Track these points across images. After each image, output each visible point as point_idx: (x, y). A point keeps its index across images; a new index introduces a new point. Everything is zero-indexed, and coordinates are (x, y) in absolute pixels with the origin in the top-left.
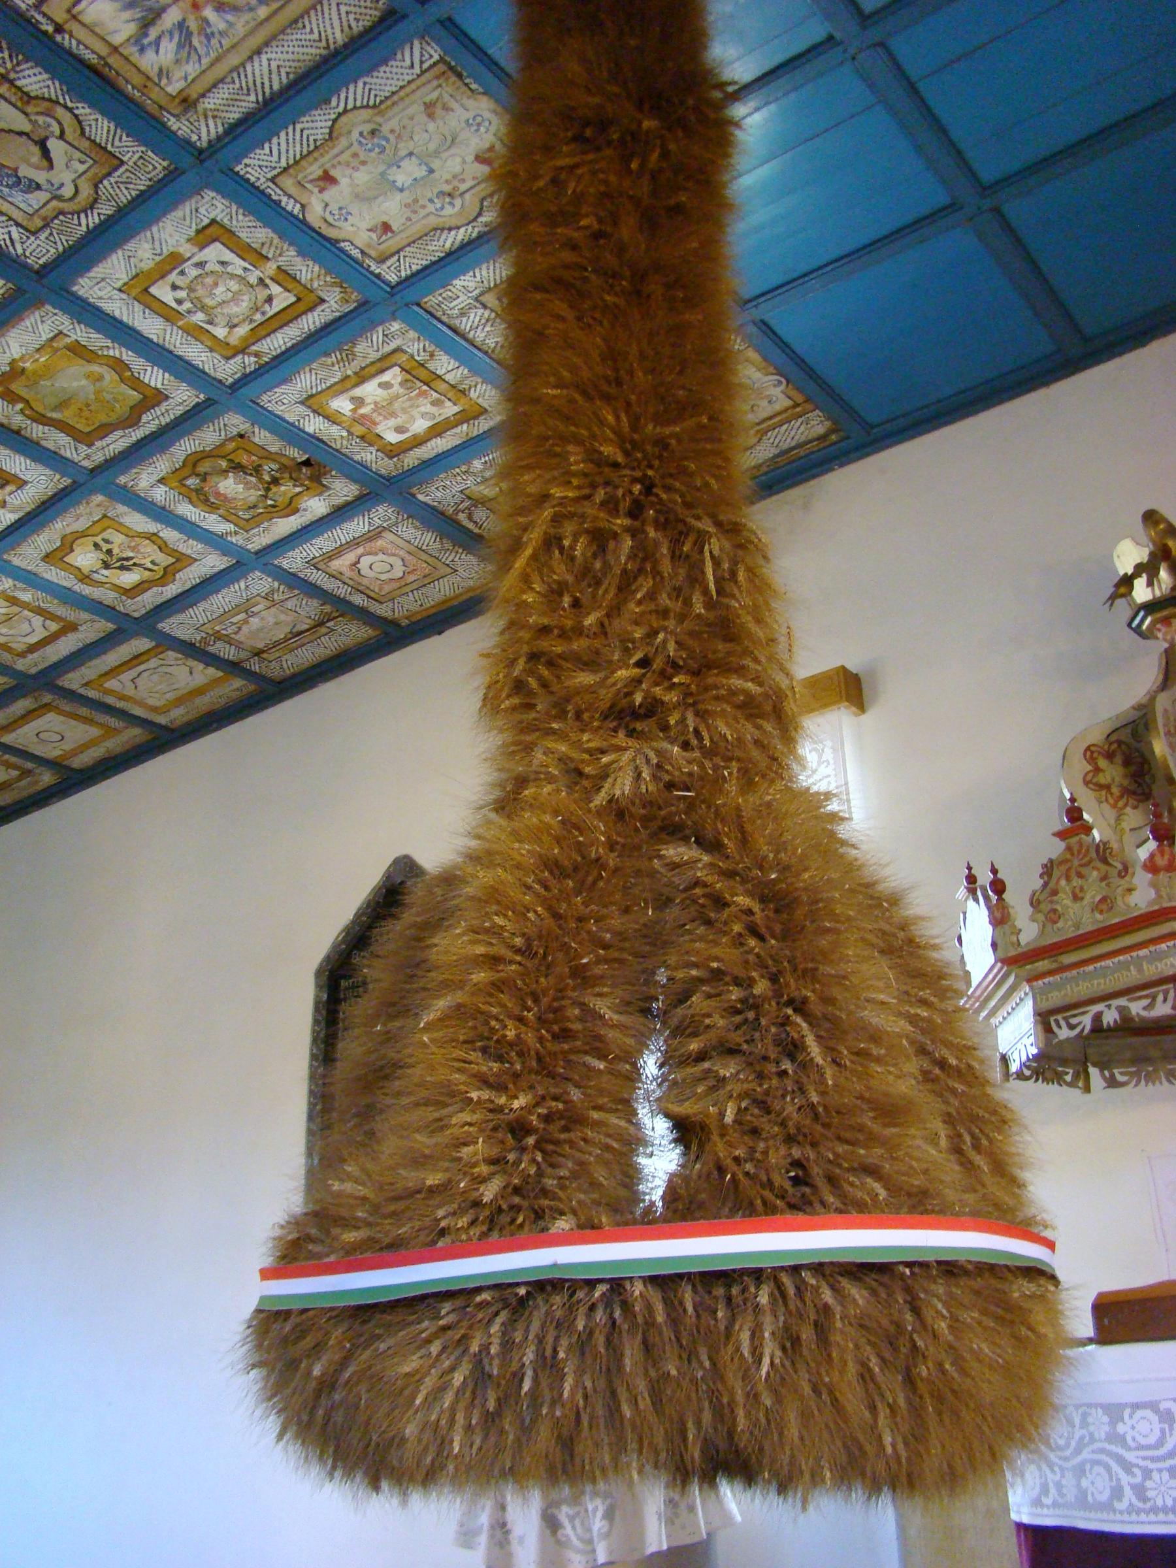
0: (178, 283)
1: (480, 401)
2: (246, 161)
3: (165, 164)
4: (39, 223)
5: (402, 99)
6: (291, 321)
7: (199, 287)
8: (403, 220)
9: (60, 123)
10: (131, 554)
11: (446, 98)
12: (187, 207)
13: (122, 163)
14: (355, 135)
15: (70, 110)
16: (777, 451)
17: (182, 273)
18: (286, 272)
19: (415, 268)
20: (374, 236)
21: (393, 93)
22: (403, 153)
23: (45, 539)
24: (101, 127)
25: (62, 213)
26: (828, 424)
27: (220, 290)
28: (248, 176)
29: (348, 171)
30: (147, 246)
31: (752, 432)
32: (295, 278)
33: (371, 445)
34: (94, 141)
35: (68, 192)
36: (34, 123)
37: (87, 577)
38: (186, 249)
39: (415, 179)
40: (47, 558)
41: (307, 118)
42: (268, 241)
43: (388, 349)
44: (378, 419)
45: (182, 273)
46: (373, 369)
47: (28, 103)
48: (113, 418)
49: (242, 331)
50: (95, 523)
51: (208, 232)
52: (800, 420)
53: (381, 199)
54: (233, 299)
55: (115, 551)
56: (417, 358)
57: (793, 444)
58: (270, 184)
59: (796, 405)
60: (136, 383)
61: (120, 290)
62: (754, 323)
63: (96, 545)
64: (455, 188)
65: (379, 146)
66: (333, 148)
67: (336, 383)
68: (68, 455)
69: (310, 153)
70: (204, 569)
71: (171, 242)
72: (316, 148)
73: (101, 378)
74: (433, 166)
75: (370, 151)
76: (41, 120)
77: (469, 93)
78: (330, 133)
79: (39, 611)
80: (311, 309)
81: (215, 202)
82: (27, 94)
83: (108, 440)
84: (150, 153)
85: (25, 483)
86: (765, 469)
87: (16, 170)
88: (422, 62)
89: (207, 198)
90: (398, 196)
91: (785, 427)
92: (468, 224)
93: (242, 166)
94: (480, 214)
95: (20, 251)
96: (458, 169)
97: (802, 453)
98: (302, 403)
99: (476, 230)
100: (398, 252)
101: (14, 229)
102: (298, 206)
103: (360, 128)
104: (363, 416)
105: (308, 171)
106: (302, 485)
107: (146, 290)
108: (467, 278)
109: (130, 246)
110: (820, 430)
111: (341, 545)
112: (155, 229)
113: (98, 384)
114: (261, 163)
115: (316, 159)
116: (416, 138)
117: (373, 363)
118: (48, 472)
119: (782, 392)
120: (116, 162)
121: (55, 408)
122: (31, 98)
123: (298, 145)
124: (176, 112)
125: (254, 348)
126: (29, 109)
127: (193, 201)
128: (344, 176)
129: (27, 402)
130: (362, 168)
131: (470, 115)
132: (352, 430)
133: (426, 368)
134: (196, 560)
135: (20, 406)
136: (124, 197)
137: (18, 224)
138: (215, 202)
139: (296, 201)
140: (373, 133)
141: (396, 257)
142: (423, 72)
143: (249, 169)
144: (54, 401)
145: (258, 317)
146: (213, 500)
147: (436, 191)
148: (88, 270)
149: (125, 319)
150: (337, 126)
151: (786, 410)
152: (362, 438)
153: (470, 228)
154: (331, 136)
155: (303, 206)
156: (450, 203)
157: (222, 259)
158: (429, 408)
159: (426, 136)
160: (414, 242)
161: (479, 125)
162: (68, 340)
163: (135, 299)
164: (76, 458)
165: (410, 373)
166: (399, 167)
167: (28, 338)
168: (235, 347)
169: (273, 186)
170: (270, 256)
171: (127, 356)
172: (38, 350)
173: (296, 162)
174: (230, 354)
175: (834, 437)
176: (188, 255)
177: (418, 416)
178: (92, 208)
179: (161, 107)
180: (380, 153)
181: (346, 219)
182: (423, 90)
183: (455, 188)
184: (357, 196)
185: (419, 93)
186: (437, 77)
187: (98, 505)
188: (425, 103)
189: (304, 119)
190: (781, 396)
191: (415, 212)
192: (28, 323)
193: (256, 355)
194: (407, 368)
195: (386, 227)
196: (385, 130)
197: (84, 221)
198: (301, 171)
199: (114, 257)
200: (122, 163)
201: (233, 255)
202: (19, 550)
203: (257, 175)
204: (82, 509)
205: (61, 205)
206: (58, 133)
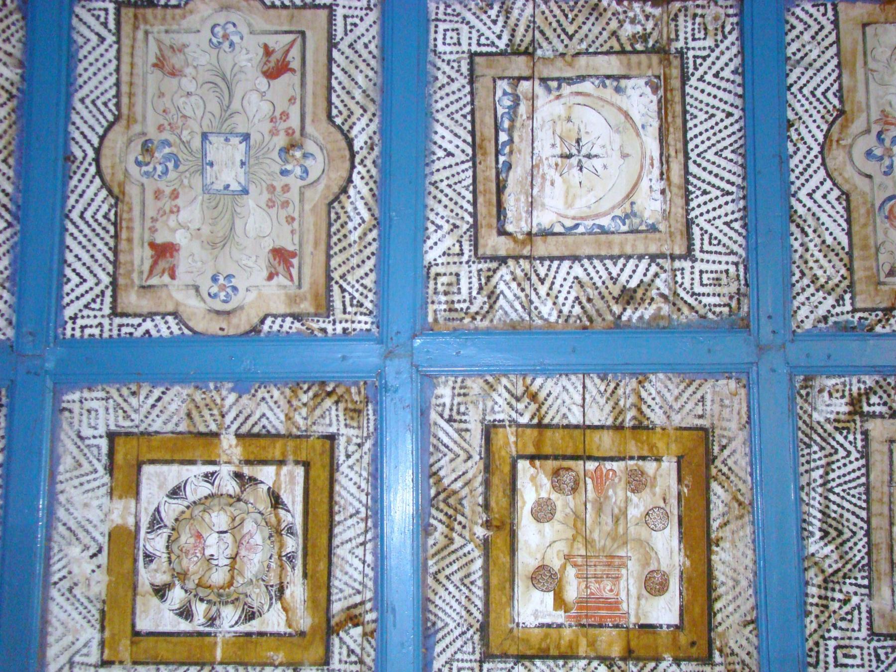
0: (162, 578)
1: (677, 420)
2: (69, 312)
5: (131, 84)
6: (331, 514)
7: (185, 562)
8: (287, 228)
11: (167, 39)
12: (67, 442)
14: (134, 170)
18: (250, 435)
19: (368, 281)
20: (281, 280)
21: (118, 84)
22: (196, 143)
27: (214, 545)
28: (87, 331)
29: (172, 222)
30: (75, 551)
32: (269, 435)
33: (658, 659)
39: (243, 164)
41: (73, 198)
42: (192, 406)
43: (476, 439)
44: (605, 589)
45: (149, 558)
46: (499, 500)
49: (297, 591)
51: (119, 458)
53: (239, 224)
54: (238, 544)
56: (524, 420)
58: (117, 321)
61: (105, 663)
64: (289, 132)
65: (168, 158)
66: (131, 210)
67: (486, 569)
69: (116, 236)
71: (95, 515)
72: (115, 224)
74: (241, 129)
75: (166, 172)
77: (178, 11)
78: (110, 192)
80: (333, 468)
81: (88, 405)
88: (105, 25)
89: (76, 407)
90: (250, 202)
92: (353, 167)
93: (69, 326)
94: (350, 143)
96: (266, 107)
98: (487, 656)
99: (368, 162)
100: (329, 279)
102: (170, 319)
103: (131, 159)
104: (583, 603)
105: (137, 262)
107: (136, 634)
108: (434, 238)
109: (57, 571)
112: (61, 513)
114: (84, 301)
115: (130, 240)
116: (188, 112)
117: (487, 483)
123: (96, 240)
125: (337, 607)
127: (65, 426)
128: (174, 231)
130: (179, 202)
131: (206, 34)
132: (603, 650)
133: (548, 426)
138: (88, 405)
139: (164, 315)
140: (147, 148)
141: (336, 288)
142: (118, 33)
143: (80, 322)
145: (292, 544)
147: (275, 155)
150: (108, 178)
152: (629, 655)
153: (359, 168)
154: (117, 197)
155: (175, 314)
156: (305, 156)
157: (170, 486)
158: (638, 505)
159: (193, 99)
160: (329, 247)
161: (226, 37)
163: (135, 663)
165: (546, 457)
166: (211, 164)
168: (313, 628)
169: (125, 320)
170: (213, 427)
173: (115, 263)
174: (321, 651)
176: (131, 521)
177: (644, 532)
180: (176, 166)
181: (235, 289)
182: (139, 52)
183: (289, 132)
184: (213, 245)
185: (138, 61)
186: (136, 28)
188: (155, 65)
189: (71, 202)
191: (285, 204)
193: (353, 618)
194: (531, 450)
195: (281, 256)
196: (152, 133)
198: (130, 272)
199: (54, 608)
201: (175, 468)
203: (95, 322)
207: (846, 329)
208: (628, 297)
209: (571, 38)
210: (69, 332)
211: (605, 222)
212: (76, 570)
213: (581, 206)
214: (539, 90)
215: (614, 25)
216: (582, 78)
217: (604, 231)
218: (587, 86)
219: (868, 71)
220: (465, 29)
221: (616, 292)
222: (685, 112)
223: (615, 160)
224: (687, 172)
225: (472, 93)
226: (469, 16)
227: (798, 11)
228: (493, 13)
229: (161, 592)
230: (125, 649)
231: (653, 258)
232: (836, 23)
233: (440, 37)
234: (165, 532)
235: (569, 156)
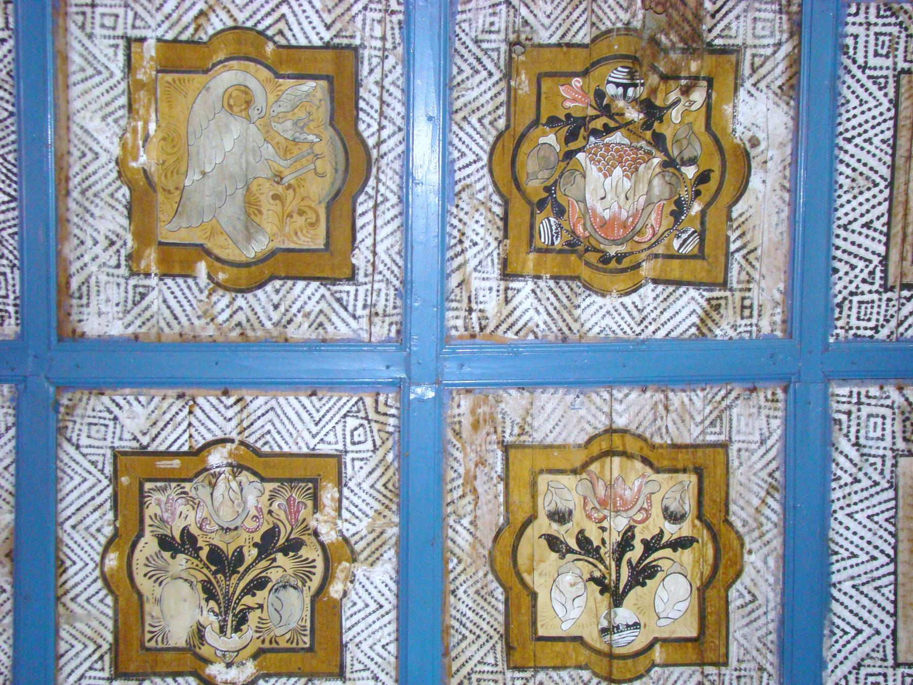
10: (620, 523)
50: (505, 479)
55: (594, 536)
63: (553, 543)
70: (757, 460)
85: (338, 458)
106: (695, 79)
111: (891, 185)
113: (254, 113)
121: (250, 228)
134: (724, 446)
135: (202, 268)
144: (231, 213)
146: (612, 250)
187: (476, 426)
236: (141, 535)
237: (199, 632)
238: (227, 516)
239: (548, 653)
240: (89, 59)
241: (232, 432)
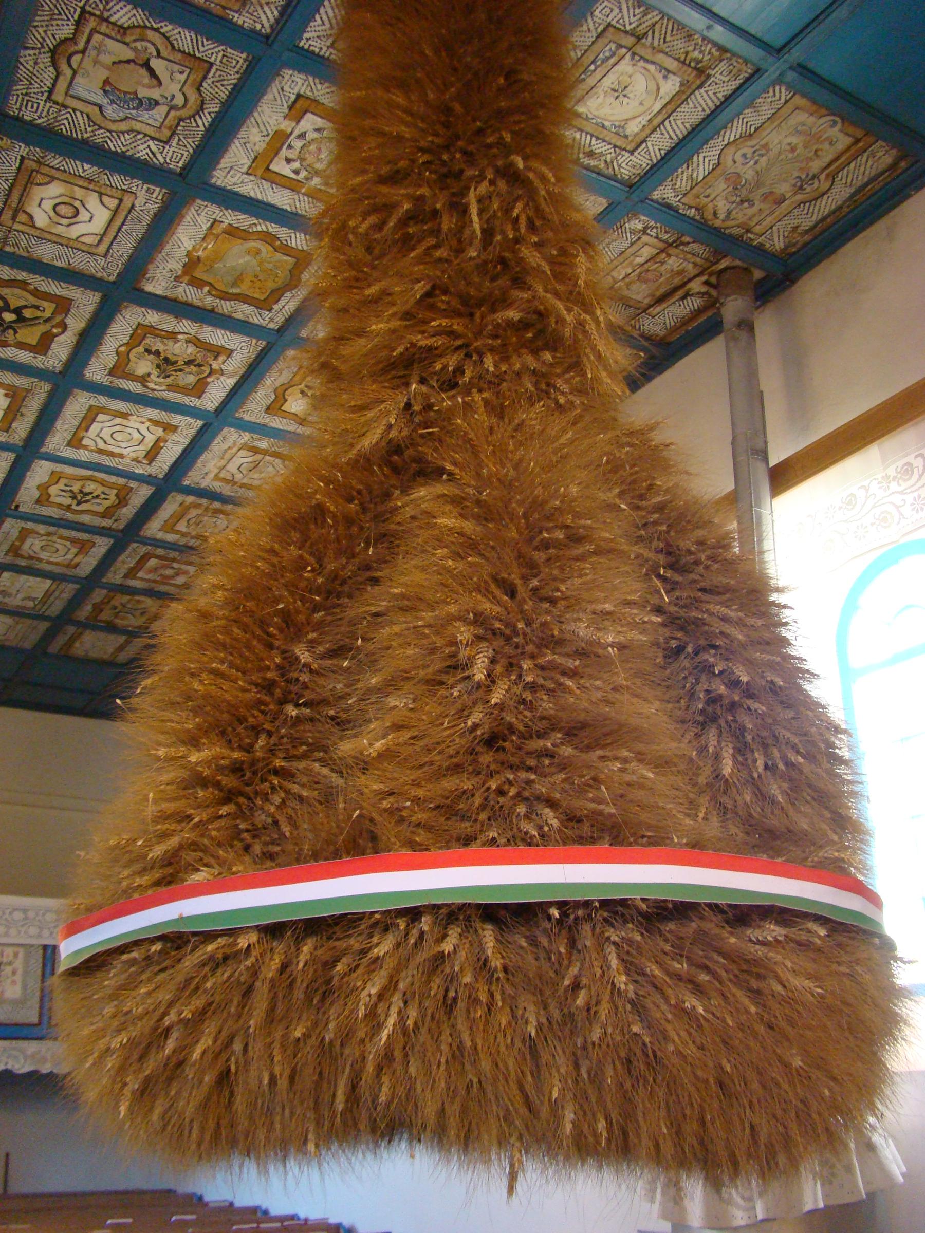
0: (291, 156)
2: (306, 35)
3: (244, 56)
4: (167, 133)
9: (153, 44)
12: (274, 89)
13: (211, 65)
15: (157, 30)
16: (853, 190)
17: (290, 147)
23: (262, 395)
24: (185, 39)
25: (181, 119)
26: (894, 152)
30: (255, 130)
31: (823, 177)
34: (184, 52)
35: (179, 100)
36: (135, 50)
37: (305, 420)
38: (287, 126)
40: (268, 409)
45: (290, 147)
47: (125, 34)
48: (279, 283)
51: (298, 106)
52: (866, 155)
57: (866, 180)
59: (857, 141)
60: (286, 250)
61: (247, 173)
62: (791, 68)
63: (302, 392)
68: (256, 321)
71: (273, 122)
73: (258, 252)
76: (138, 45)
79: (276, 455)
82: (121, 27)
83: (282, 302)
84: (229, 50)
85: (232, 351)
86: (846, 210)
87: (135, 93)
89: (287, 77)
91: (853, 165)
95: (162, 160)
97: (877, 187)
101: (151, 143)
107: (268, 169)
109: (242, 133)
110: (888, 160)
112: (256, 114)
113: (258, 257)
118: (246, 339)
119: (841, 131)
120: (206, 65)
121: (234, 284)
122: (125, 29)
124: (236, 8)
126: (128, 39)
129: (210, 284)
135: (206, 289)
136: (223, 93)
137: (153, 138)
138: (293, 78)
148: (218, 163)
149: (260, 197)
151: (848, 149)
162: (224, 226)
164: (264, 323)
167: (192, 231)
171: (273, 228)
172: (203, 239)
175: (903, 164)
176: (289, 130)
178: (202, 109)
179: (224, 8)
190: (841, 136)
192: (188, 218)
197: (200, 123)
199: (233, 146)
200: (211, 65)
202: (245, 408)
204: (281, 364)
205: (178, 113)
206: (155, 53)
207: (669, 206)
208: (591, 154)
209: (665, 42)
210: (301, 44)
211: (607, 124)
212: (251, 137)
213: (602, 112)
214: (628, 57)
215: (691, 48)
216: (653, 63)
217: (603, 127)
218: (652, 68)
219: (779, 125)
220: (616, 11)
221: (587, 149)
222: (686, 99)
223: (636, 103)
224: (663, 122)
225: (593, 43)
226: (624, 7)
227: (777, 88)
228: (637, 11)
229: (288, 161)
230: (260, 172)
231: (615, 147)
232: (786, 102)
233: (600, 8)
234: (303, 142)
235: (615, 91)
236: (139, 345)
237: (149, 375)
238: (177, 352)
239: (283, 414)
240: (194, 221)
241: (193, 332)
